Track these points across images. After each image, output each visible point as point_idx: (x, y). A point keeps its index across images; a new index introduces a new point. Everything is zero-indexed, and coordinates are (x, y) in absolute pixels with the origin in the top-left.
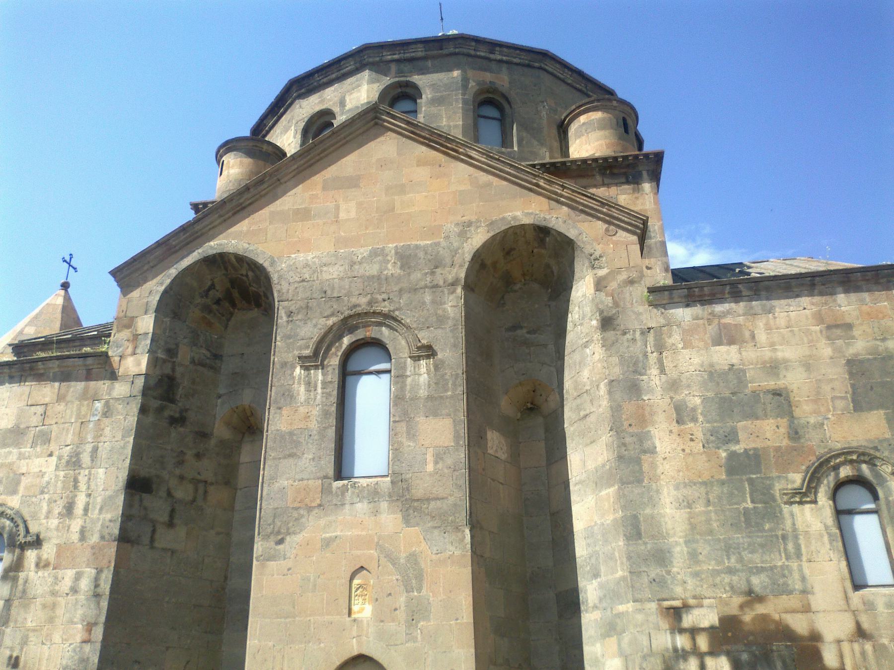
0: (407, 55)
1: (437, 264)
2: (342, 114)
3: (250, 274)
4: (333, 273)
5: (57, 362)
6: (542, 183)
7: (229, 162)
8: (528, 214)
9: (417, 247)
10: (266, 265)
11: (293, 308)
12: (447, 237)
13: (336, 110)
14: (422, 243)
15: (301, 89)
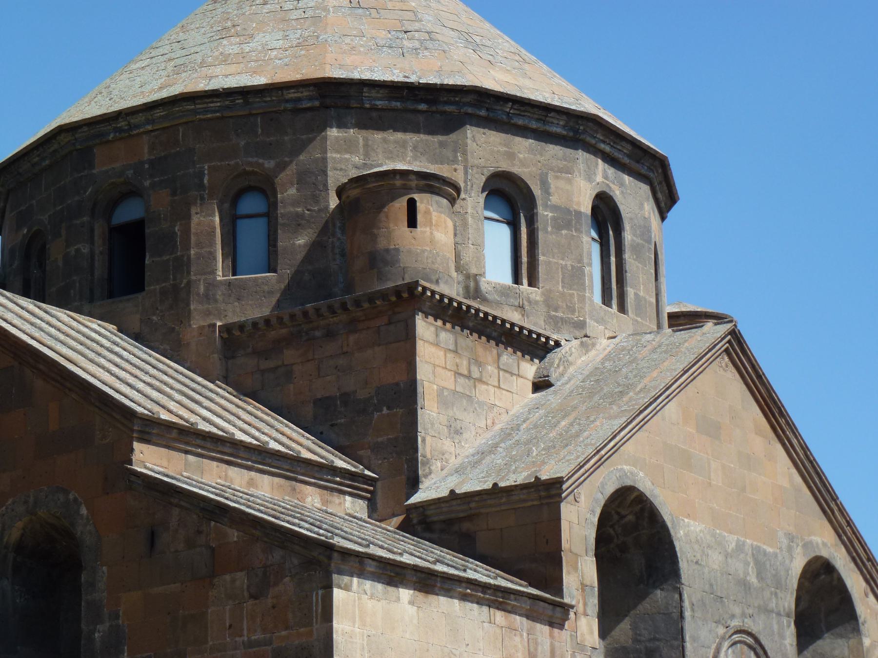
0: (617, 154)
1: (779, 585)
2: (546, 206)
3: (631, 518)
4: (715, 559)
5: (529, 602)
6: (835, 508)
7: (427, 212)
8: (824, 544)
9: (765, 553)
10: (669, 524)
11: (694, 600)
12: (781, 548)
13: (537, 191)
14: (770, 550)
15: (480, 108)
